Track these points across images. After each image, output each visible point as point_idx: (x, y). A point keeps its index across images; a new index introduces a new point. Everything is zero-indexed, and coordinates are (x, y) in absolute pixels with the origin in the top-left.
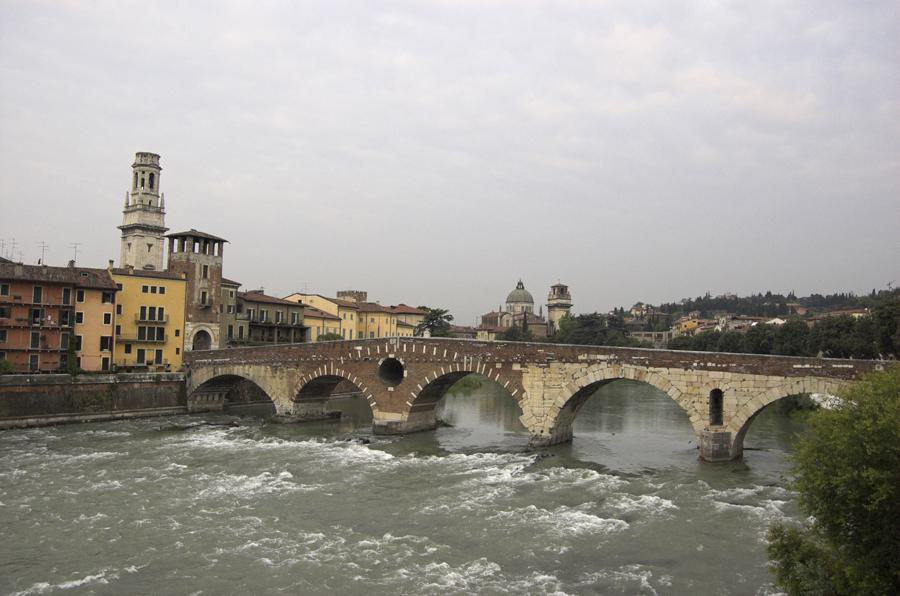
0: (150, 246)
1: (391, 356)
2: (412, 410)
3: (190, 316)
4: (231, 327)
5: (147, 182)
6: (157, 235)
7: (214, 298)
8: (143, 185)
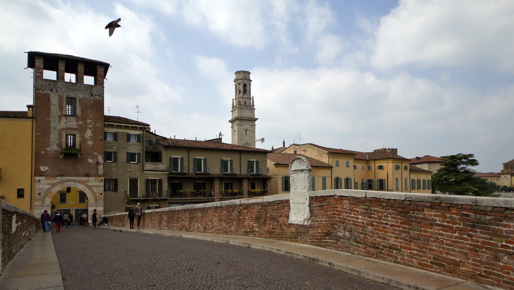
0: (246, 130)
3: (43, 169)
4: (134, 182)
5: (242, 90)
7: (90, 143)
8: (240, 93)
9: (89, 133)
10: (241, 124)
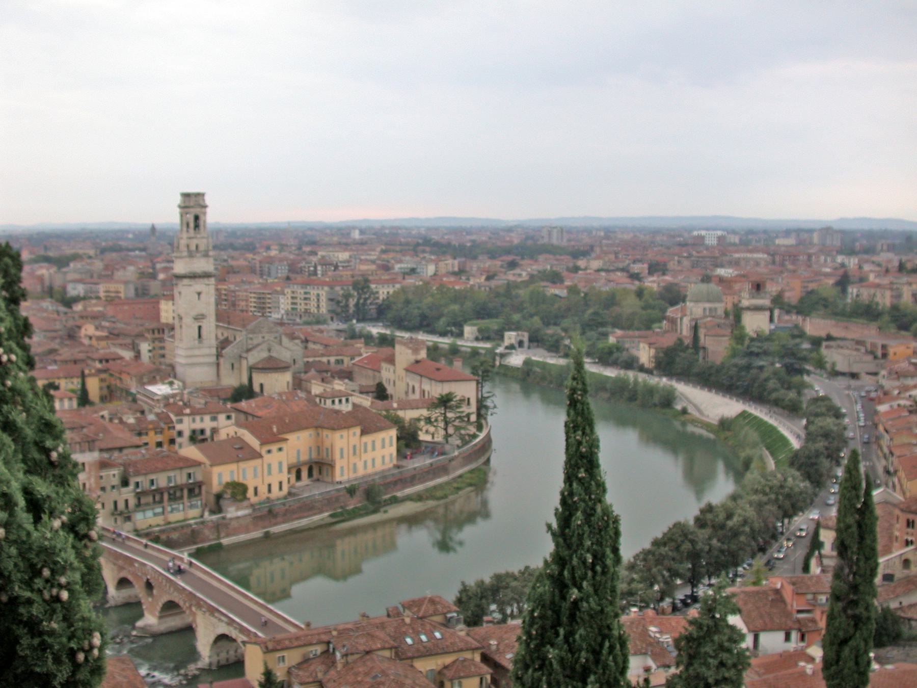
0: (199, 294)
1: (149, 577)
2: (160, 618)
4: (115, 503)
5: (192, 225)
6: (206, 281)
9: (93, 480)
10: (190, 283)
